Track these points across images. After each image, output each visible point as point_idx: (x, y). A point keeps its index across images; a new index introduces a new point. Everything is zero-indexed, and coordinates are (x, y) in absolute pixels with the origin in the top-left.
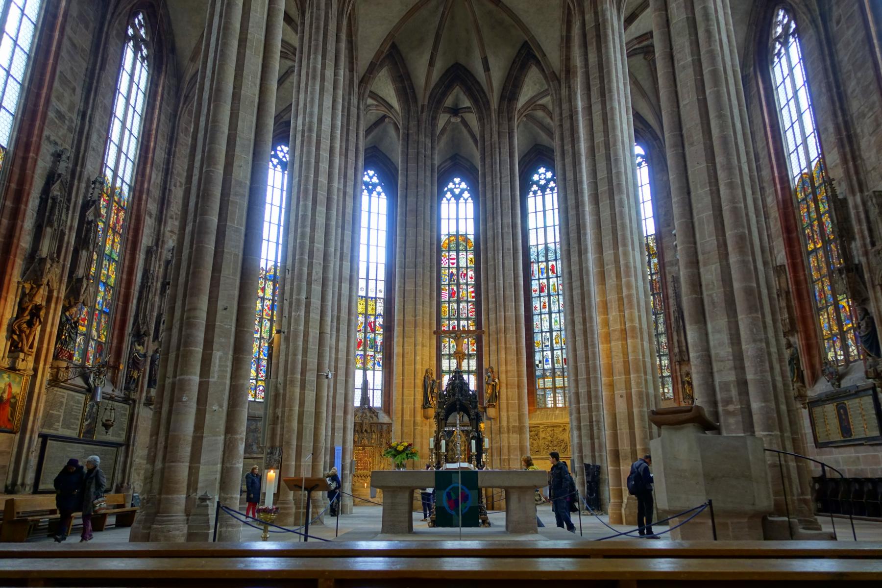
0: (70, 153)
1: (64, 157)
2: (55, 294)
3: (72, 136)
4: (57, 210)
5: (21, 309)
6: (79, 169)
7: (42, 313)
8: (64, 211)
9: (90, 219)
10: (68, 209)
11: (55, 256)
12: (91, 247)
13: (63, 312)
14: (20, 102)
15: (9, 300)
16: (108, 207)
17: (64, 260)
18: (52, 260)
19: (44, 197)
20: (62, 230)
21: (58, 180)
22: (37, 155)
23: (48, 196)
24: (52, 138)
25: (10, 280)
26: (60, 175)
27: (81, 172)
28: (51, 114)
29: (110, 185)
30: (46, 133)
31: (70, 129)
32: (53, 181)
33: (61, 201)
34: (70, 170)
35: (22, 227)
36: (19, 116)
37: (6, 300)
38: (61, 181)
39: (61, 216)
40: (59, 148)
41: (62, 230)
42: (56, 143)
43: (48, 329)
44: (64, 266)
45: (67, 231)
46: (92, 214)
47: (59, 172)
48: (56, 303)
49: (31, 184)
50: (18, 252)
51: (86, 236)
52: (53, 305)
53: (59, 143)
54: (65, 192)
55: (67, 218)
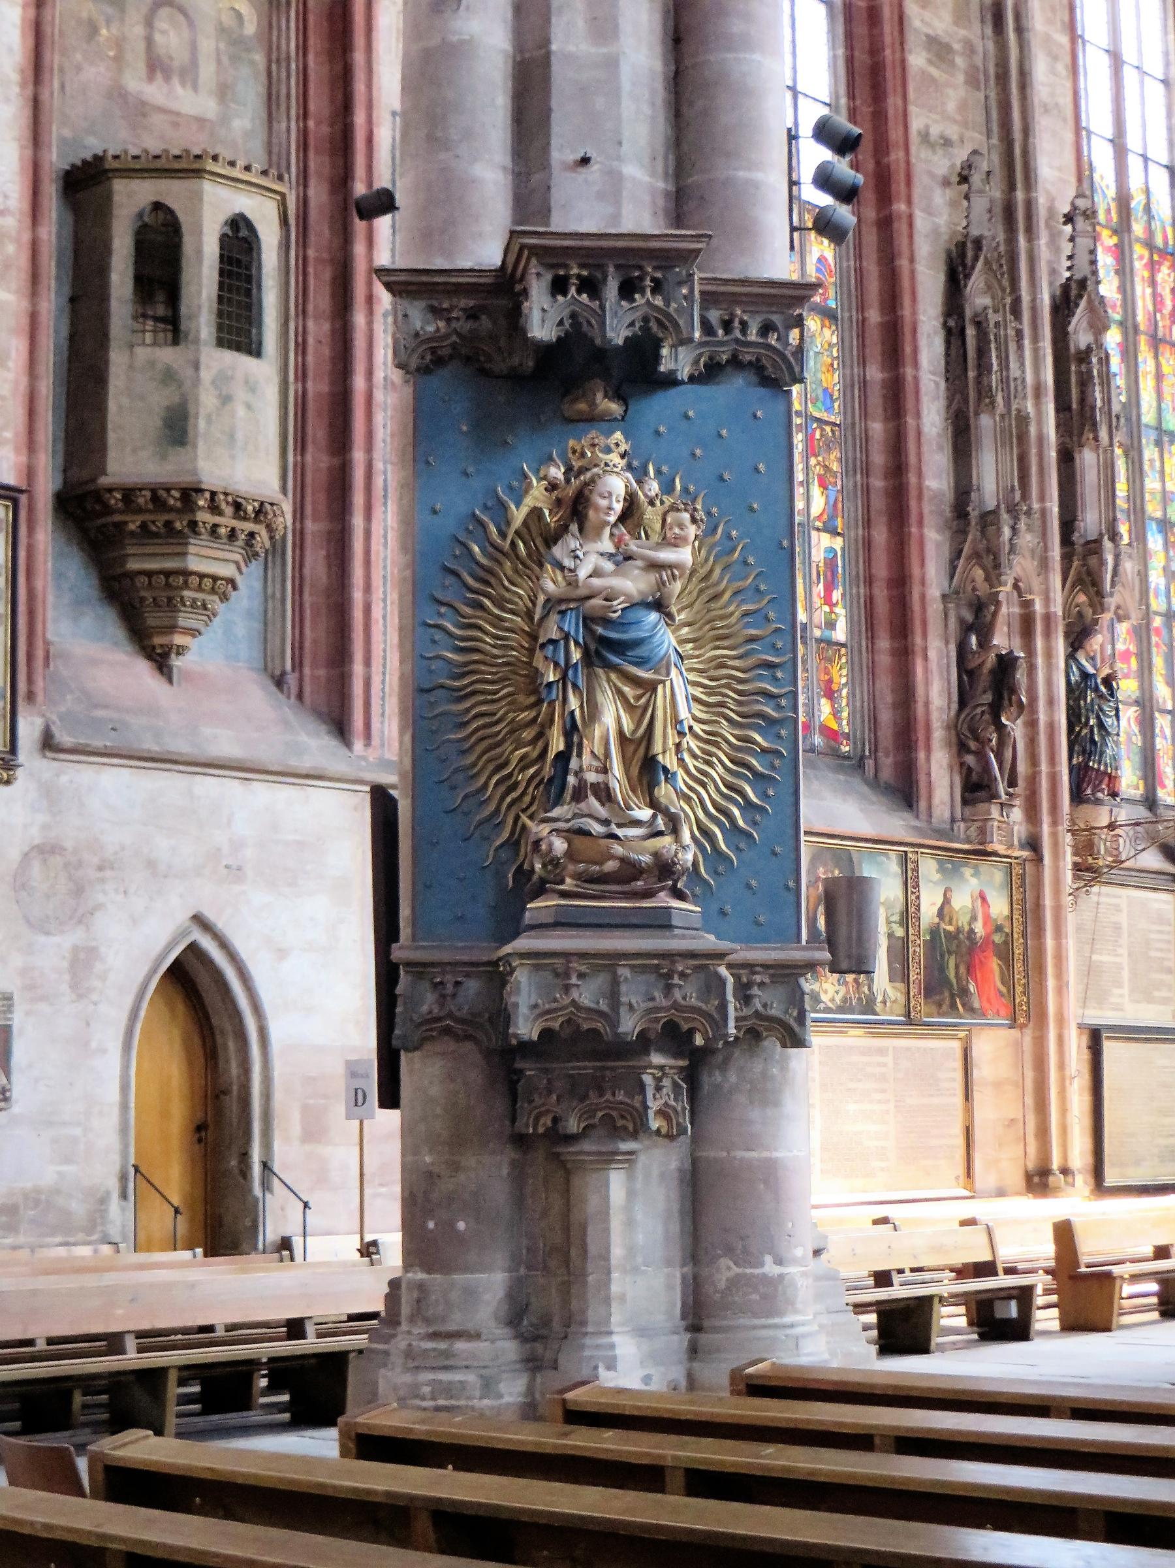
0: (991, 161)
1: (976, 179)
2: (1038, 607)
3: (981, 95)
4: (994, 354)
5: (966, 671)
6: (1020, 195)
7: (1021, 676)
8: (1012, 347)
9: (1083, 346)
10: (1019, 334)
11: (1018, 495)
12: (1103, 434)
13: (1071, 657)
14: (835, 57)
15: (932, 654)
16: (1124, 270)
17: (1042, 498)
18: (1013, 510)
19: (951, 323)
20: (1019, 411)
21: (976, 258)
22: (909, 202)
23: (961, 316)
24: (935, 131)
25: (923, 597)
26: (978, 243)
27: (1029, 205)
28: (917, 60)
29: (1112, 192)
30: (917, 123)
31: (973, 81)
32: (964, 265)
33: (997, 324)
34: (998, 210)
35: (919, 433)
36: (843, 101)
37: (926, 658)
38: (987, 262)
39: (1008, 368)
40: (961, 155)
41: (1019, 411)
42: (947, 143)
43: (1042, 717)
44: (1044, 513)
45: (1030, 407)
46: (1084, 324)
47: (975, 232)
48: (1048, 634)
49: (914, 299)
50: (926, 509)
51: (1082, 400)
52: (1039, 643)
53: (955, 137)
54: (1003, 290)
55: (1023, 372)
